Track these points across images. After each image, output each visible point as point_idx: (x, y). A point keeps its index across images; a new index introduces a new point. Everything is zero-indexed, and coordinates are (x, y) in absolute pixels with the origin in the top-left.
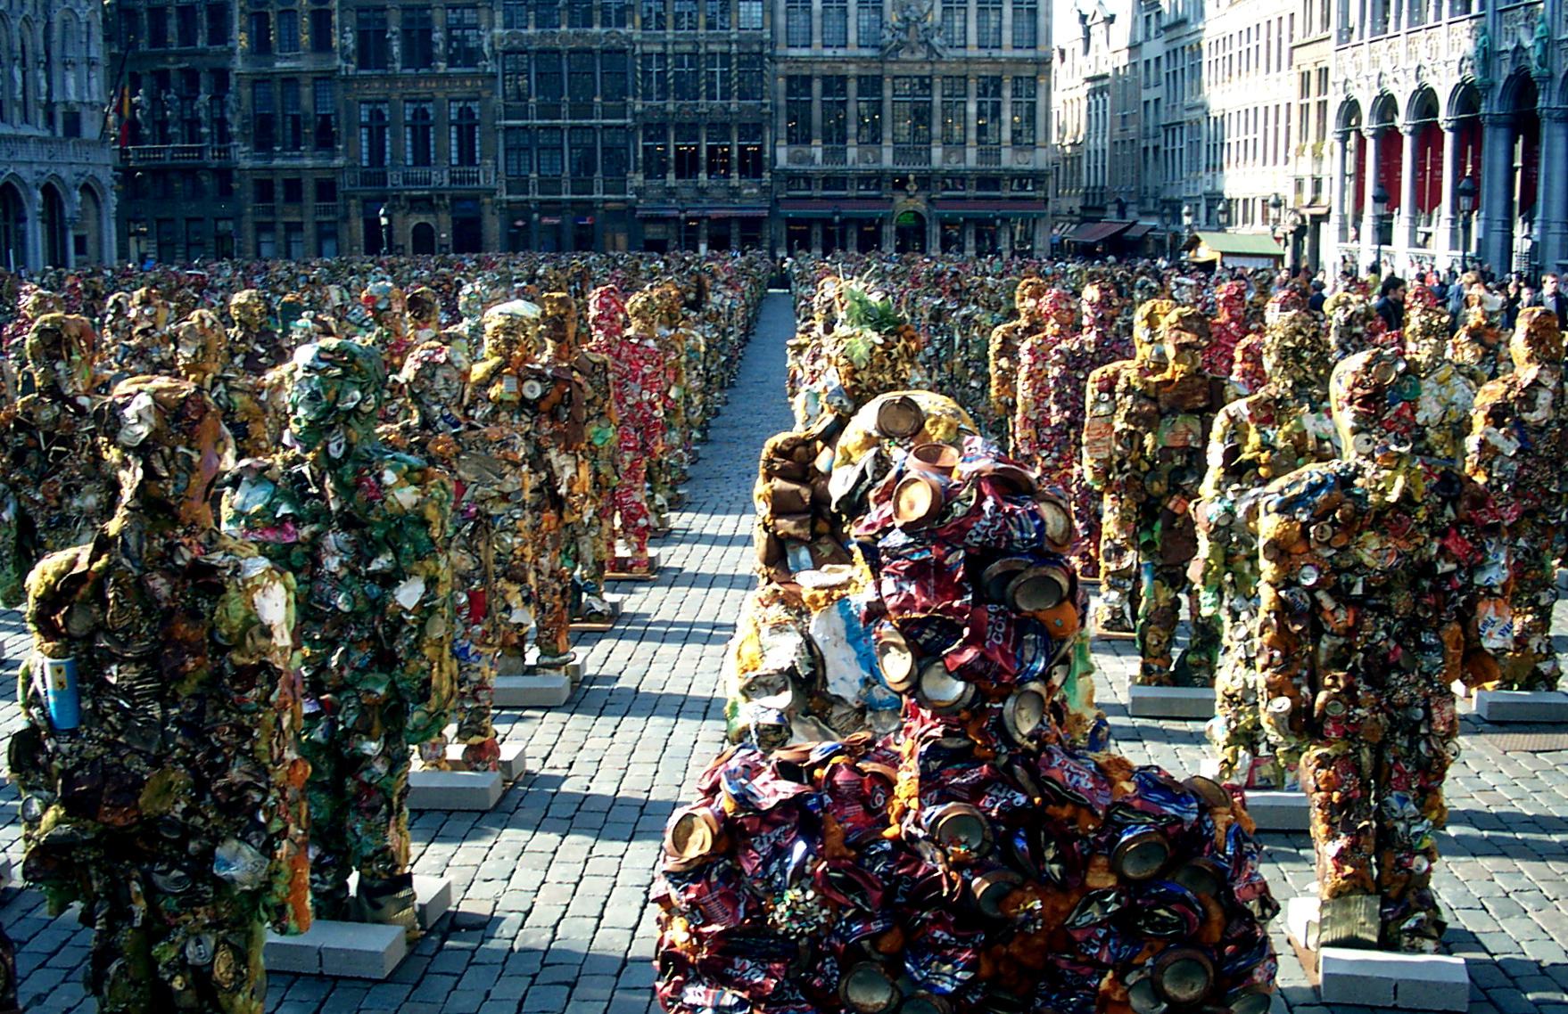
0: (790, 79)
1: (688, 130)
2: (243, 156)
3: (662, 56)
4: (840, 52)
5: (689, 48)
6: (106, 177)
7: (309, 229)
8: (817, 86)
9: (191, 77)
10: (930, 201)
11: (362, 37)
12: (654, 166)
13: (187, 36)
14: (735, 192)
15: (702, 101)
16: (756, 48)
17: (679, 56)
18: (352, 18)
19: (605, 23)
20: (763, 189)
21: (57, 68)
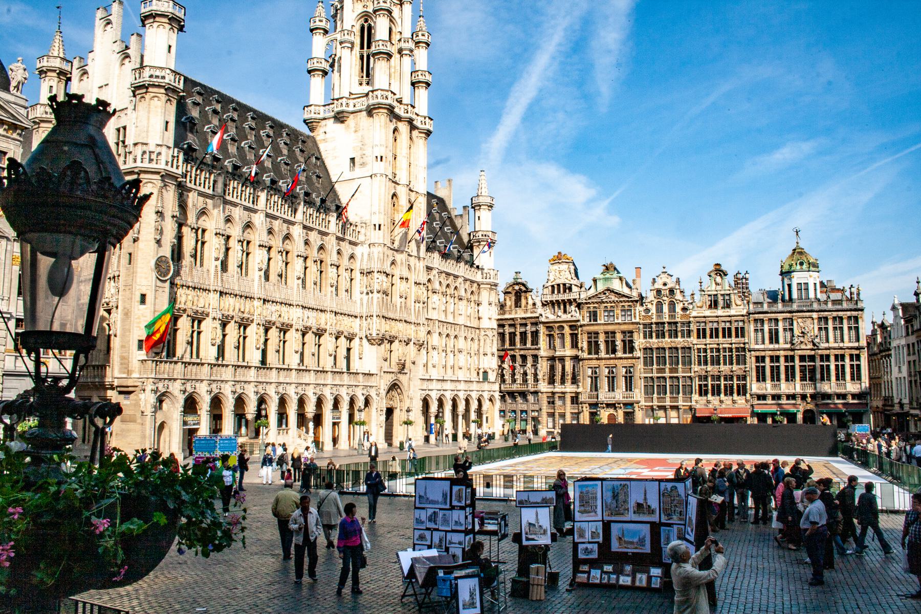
0: (757, 357)
2: (543, 387)
3: (705, 350)
4: (777, 346)
5: (715, 346)
6: (497, 395)
8: (768, 360)
9: (524, 358)
10: (817, 405)
11: (589, 343)
12: (703, 392)
15: (722, 366)
16: (742, 345)
17: (712, 349)
18: (585, 337)
19: (683, 336)
20: (747, 401)
21: (481, 355)
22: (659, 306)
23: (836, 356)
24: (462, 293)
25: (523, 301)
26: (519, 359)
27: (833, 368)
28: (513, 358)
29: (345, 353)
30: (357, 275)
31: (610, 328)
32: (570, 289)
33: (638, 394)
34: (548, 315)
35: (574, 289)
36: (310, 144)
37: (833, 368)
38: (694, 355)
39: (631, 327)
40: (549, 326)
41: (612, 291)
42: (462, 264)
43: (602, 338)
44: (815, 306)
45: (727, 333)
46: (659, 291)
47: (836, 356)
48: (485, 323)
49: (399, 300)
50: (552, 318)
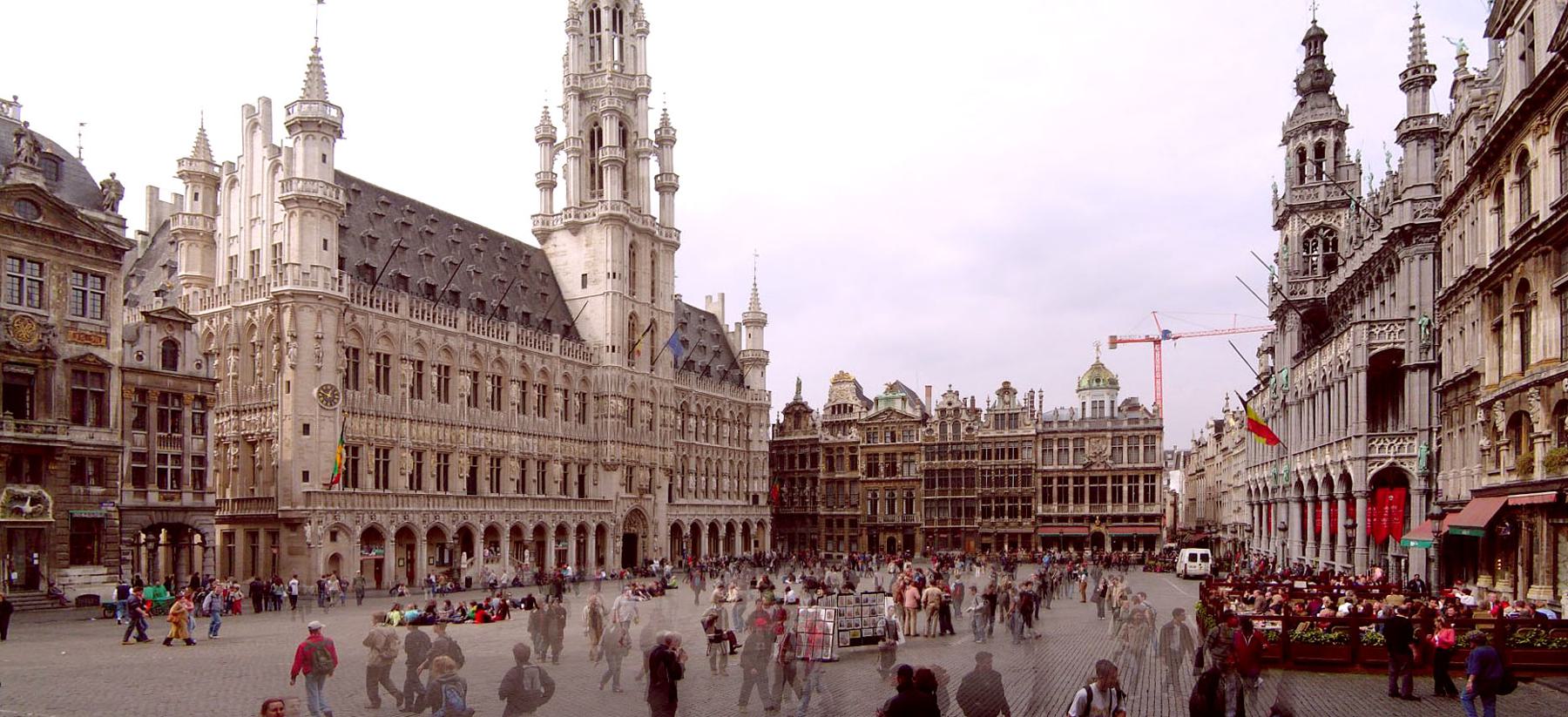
0: (1044, 480)
1: (1000, 500)
6: (768, 519)
9: (803, 481)
11: (869, 466)
12: (986, 513)
13: (803, 465)
24: (727, 416)
25: (803, 423)
27: (1125, 489)
28: (792, 481)
29: (576, 479)
34: (825, 436)
36: (535, 260)
37: (1125, 489)
40: (829, 448)
41: (893, 411)
43: (881, 460)
48: (755, 447)
50: (831, 439)
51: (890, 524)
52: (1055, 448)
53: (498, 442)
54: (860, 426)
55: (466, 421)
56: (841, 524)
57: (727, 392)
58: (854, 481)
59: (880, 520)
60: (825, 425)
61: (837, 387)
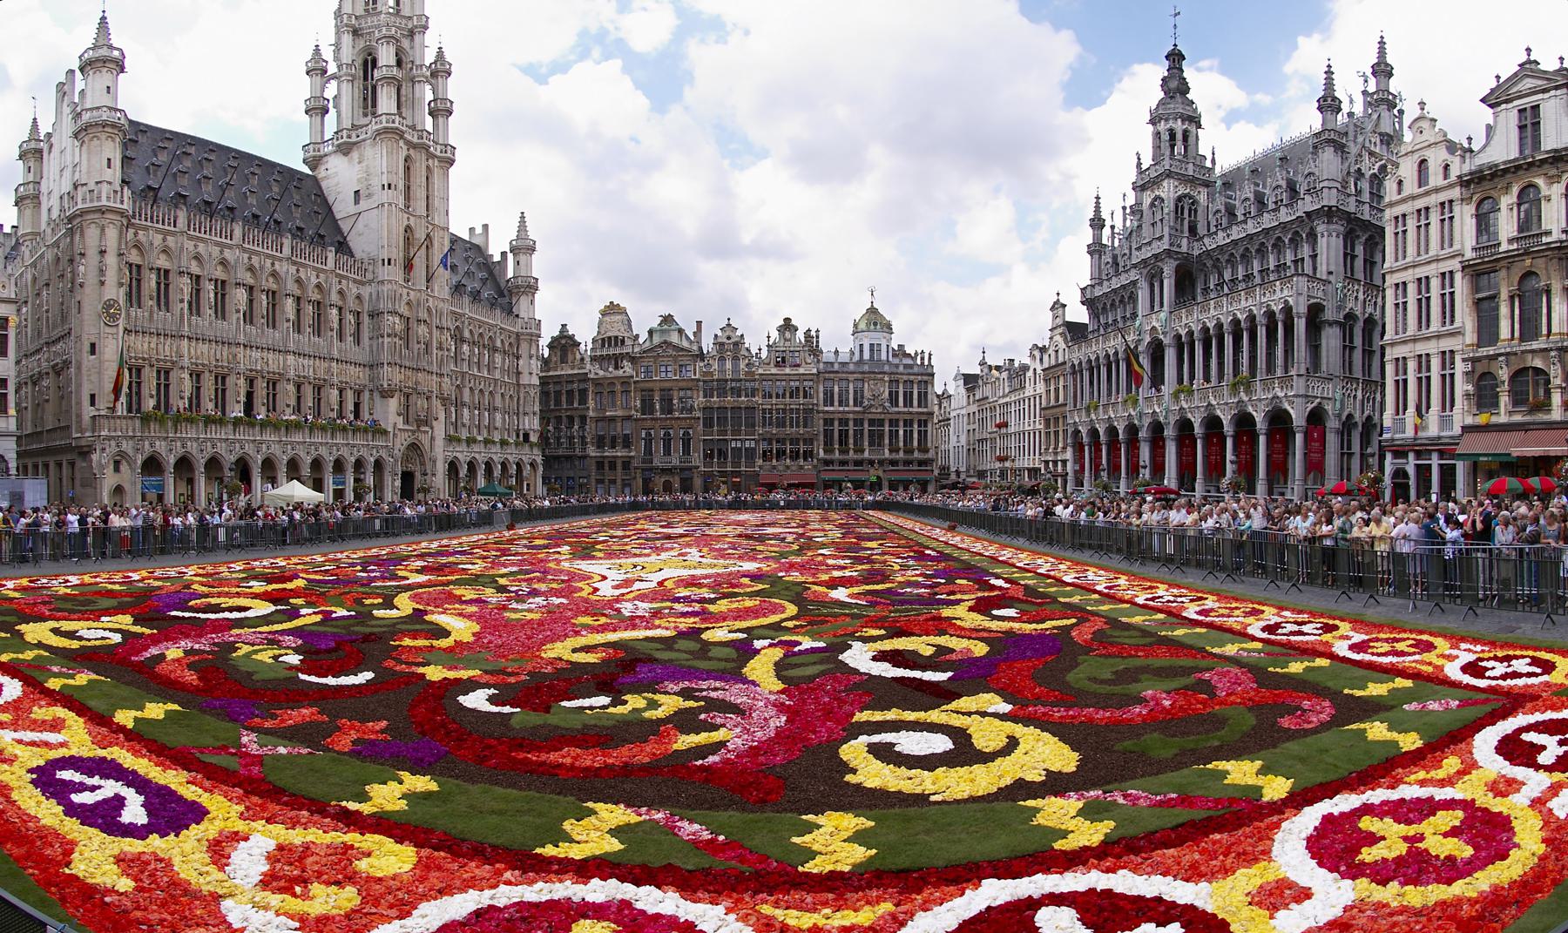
0: (825, 421)
2: (592, 451)
6: (539, 459)
7: (619, 482)
9: (571, 419)
11: (643, 401)
12: (766, 456)
13: (570, 402)
14: (801, 467)
18: (639, 395)
22: (722, 359)
23: (905, 421)
24: (499, 344)
25: (570, 357)
26: (564, 420)
28: (559, 419)
30: (366, 319)
31: (667, 385)
32: (623, 342)
33: (697, 459)
34: (595, 371)
35: (628, 342)
38: (758, 416)
39: (690, 384)
40: (597, 383)
42: (498, 312)
44: (886, 368)
45: (794, 393)
46: (722, 344)
47: (905, 421)
48: (525, 380)
49: (416, 346)
51: (669, 466)
52: (836, 389)
53: (274, 362)
54: (633, 359)
55: (242, 339)
56: (613, 466)
57: (496, 319)
58: (629, 418)
59: (657, 463)
60: (594, 359)
61: (607, 319)
